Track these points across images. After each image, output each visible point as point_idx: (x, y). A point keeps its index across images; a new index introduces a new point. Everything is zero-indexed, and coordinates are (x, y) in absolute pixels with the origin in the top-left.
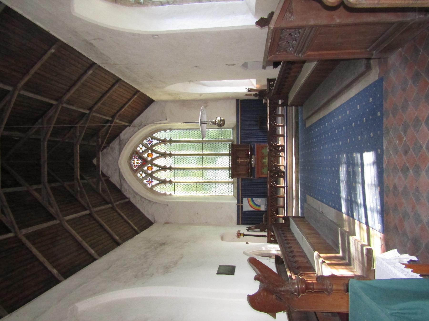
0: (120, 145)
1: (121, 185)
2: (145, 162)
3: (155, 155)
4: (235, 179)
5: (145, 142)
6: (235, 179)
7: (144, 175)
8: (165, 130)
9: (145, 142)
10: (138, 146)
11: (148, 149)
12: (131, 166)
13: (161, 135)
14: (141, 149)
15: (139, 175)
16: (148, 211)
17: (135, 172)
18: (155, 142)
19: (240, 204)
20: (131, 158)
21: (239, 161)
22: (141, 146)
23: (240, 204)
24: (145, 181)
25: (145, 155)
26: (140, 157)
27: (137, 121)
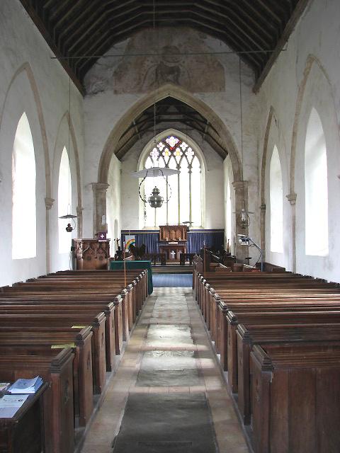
0: (187, 129)
1: (153, 131)
2: (172, 150)
3: (178, 158)
4: (159, 229)
5: (190, 149)
6: (159, 229)
7: (161, 149)
8: (200, 167)
9: (190, 149)
10: (187, 143)
11: (184, 153)
12: (168, 137)
13: (196, 163)
14: (184, 146)
15: (161, 144)
16: (130, 155)
17: (164, 142)
18: (190, 158)
19: (130, 233)
20: (176, 137)
21: (173, 232)
22: (187, 146)
23: (130, 233)
24: (155, 149)
25: (178, 150)
26: (177, 145)
27: (208, 146)
